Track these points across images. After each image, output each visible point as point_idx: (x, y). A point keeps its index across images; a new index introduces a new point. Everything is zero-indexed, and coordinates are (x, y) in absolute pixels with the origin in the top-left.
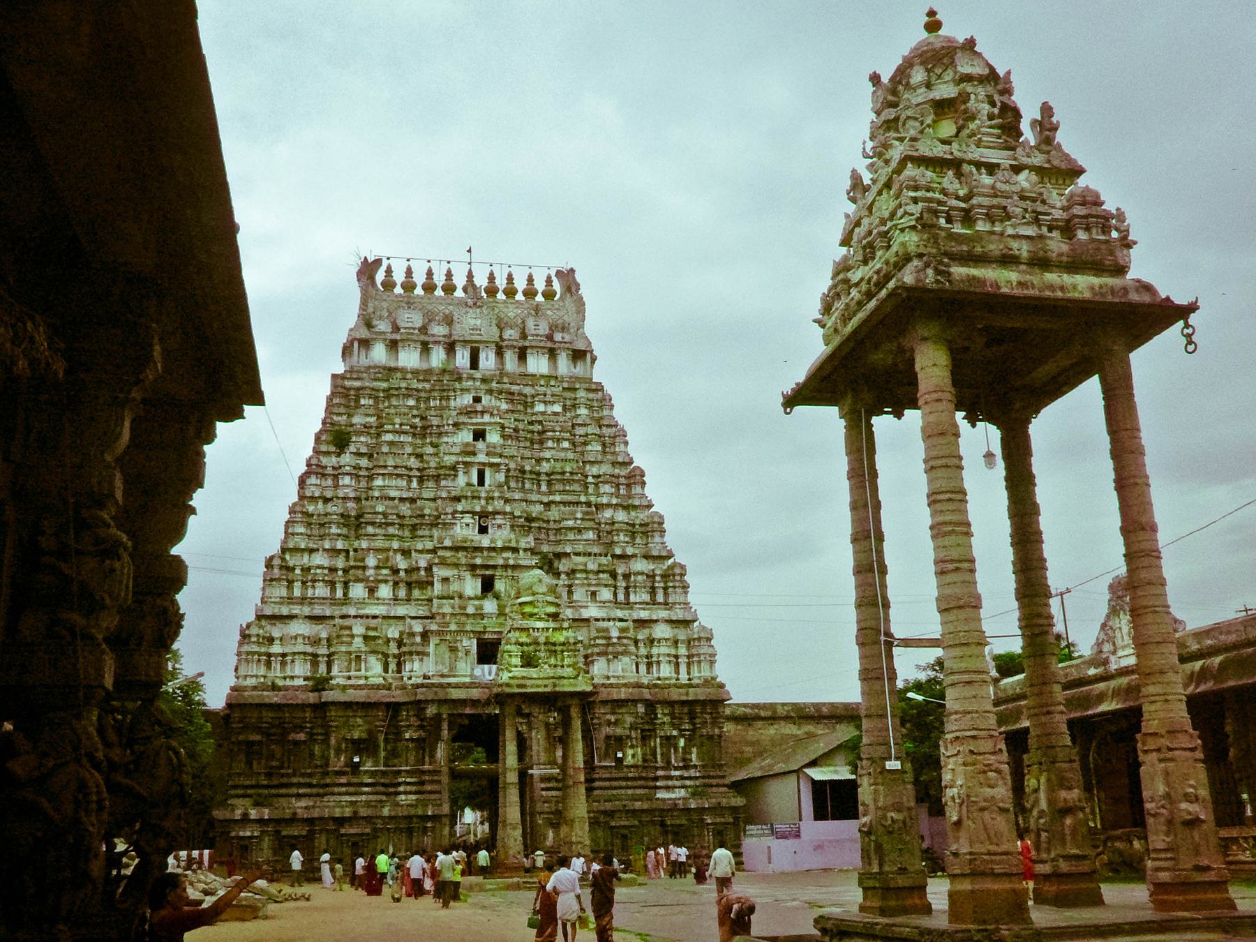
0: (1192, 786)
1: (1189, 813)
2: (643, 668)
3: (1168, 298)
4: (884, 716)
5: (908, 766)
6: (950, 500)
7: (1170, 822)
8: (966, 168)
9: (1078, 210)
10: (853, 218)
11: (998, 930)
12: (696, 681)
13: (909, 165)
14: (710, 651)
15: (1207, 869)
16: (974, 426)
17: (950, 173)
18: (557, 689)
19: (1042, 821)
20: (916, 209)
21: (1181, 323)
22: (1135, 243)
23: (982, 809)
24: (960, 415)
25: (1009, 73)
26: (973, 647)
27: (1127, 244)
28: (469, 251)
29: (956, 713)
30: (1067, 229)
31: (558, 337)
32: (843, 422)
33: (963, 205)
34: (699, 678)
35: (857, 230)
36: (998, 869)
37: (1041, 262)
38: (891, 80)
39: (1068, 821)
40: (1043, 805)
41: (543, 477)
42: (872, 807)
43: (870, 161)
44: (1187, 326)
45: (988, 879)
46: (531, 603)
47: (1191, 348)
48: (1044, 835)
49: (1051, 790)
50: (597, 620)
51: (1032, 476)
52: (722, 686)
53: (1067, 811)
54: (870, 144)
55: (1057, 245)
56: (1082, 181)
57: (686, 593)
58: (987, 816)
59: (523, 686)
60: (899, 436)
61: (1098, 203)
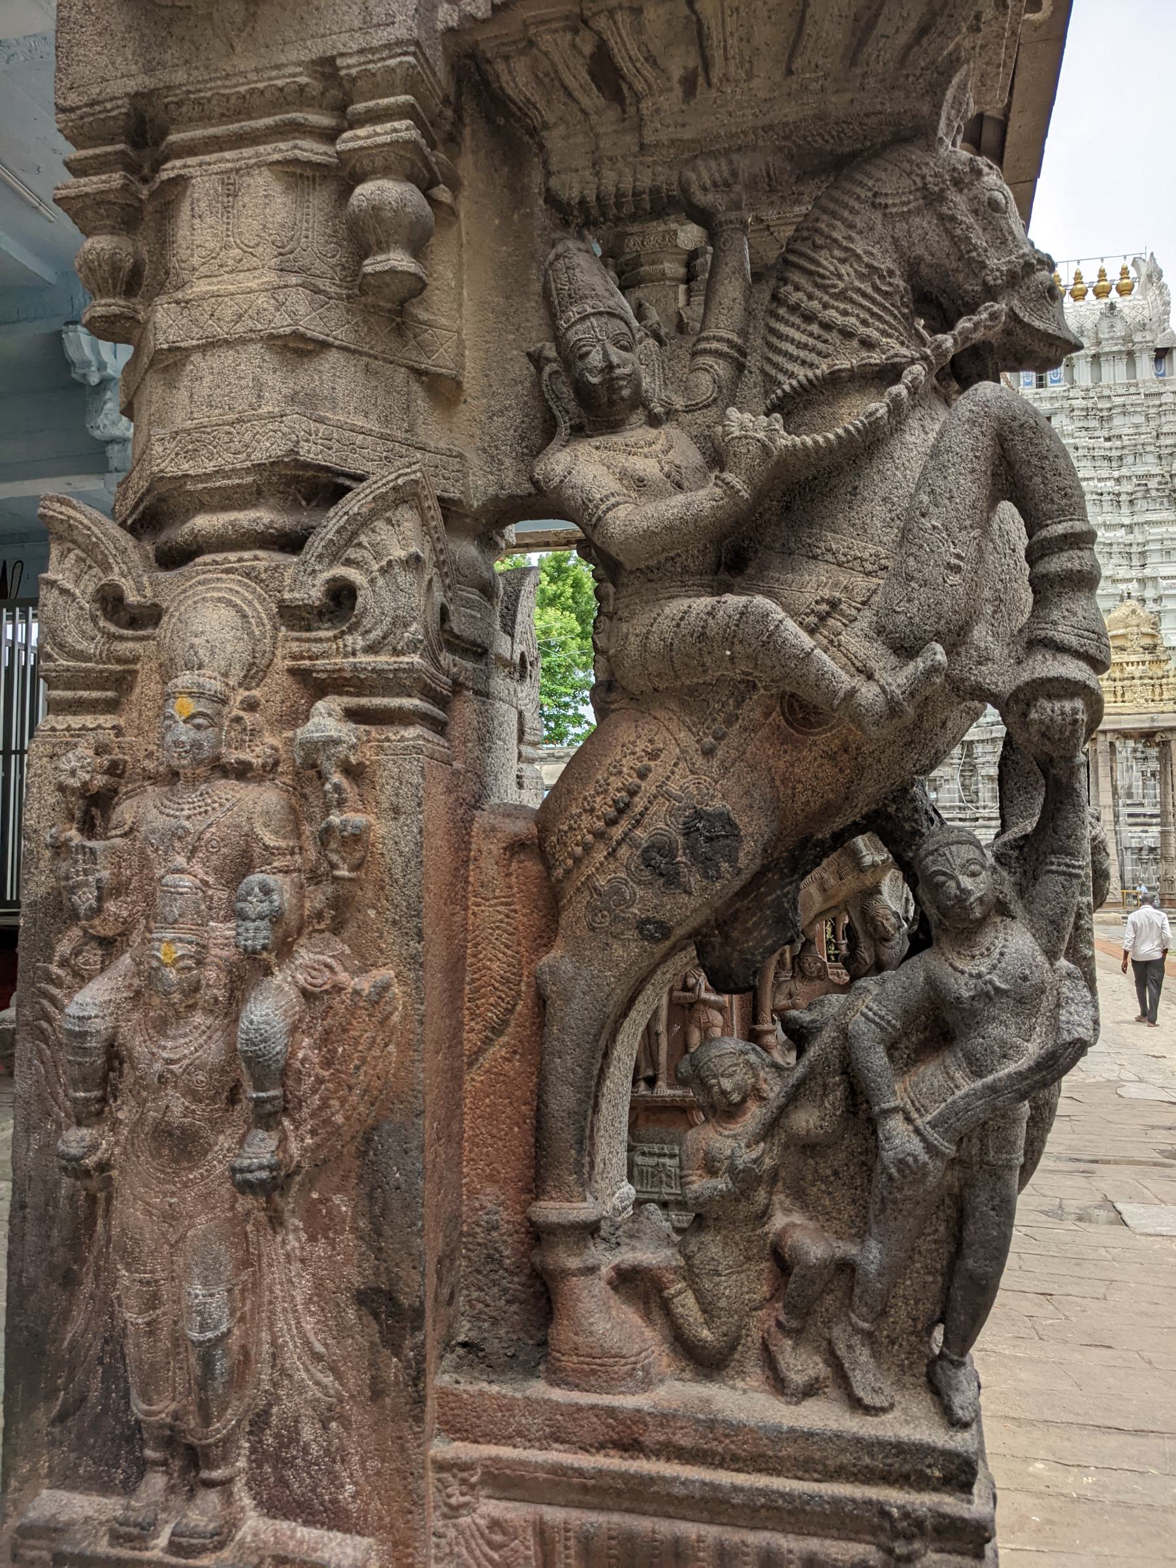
31: (1137, 338)
41: (1123, 497)
46: (1124, 636)
59: (1119, 722)
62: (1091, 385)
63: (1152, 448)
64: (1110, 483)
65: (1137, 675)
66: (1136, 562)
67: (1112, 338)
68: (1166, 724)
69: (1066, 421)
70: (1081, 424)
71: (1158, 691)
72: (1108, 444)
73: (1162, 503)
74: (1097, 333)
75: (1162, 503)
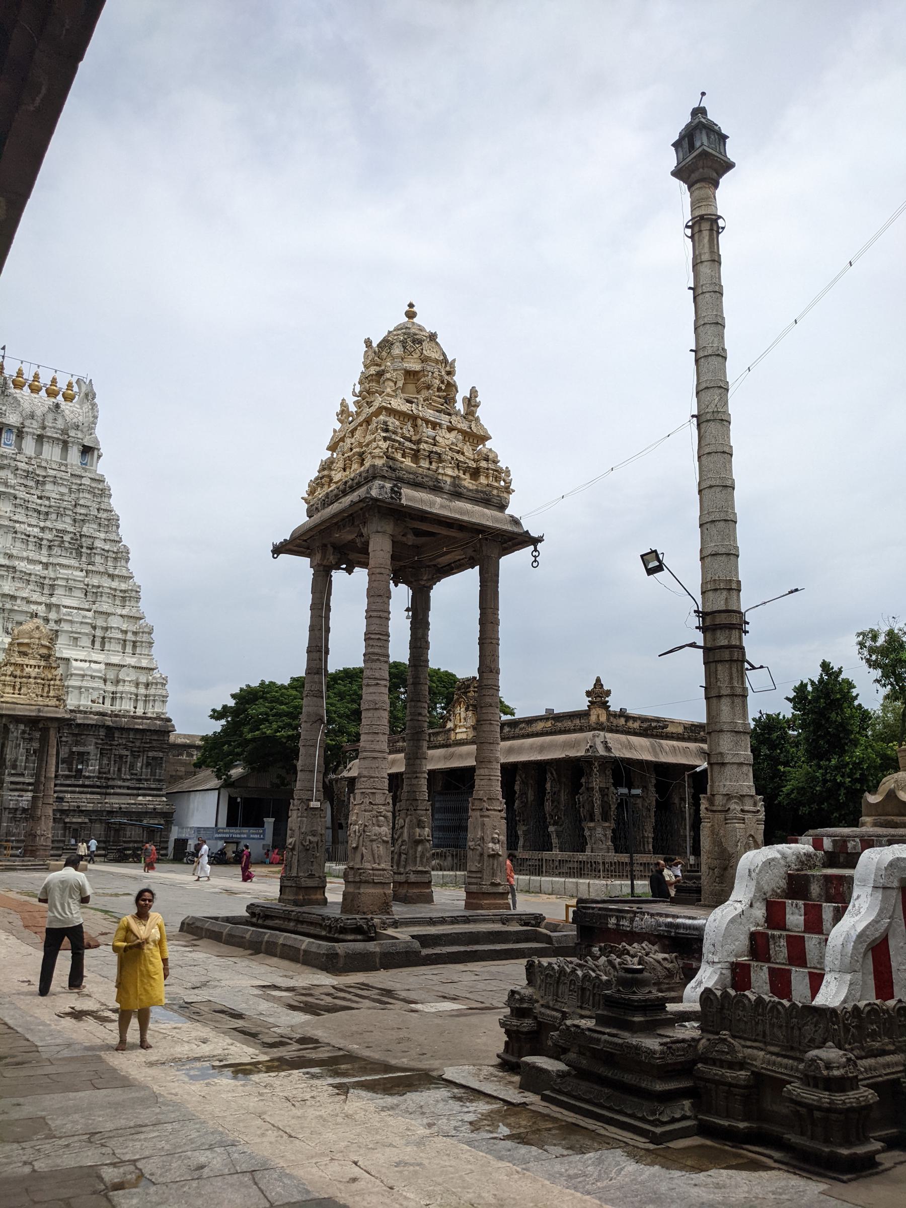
0: (496, 833)
1: (493, 850)
2: (108, 701)
3: (527, 531)
4: (313, 771)
6: (379, 639)
8: (419, 422)
9: (483, 464)
11: (372, 919)
12: (149, 715)
13: (384, 413)
14: (164, 693)
15: (499, 884)
17: (409, 424)
18: (41, 714)
19: (403, 847)
21: (532, 548)
22: (514, 491)
23: (372, 841)
25: (454, 360)
26: (380, 735)
27: (508, 490)
28: (4, 348)
29: (365, 777)
30: (475, 473)
31: (72, 433)
32: (312, 571)
33: (415, 447)
34: (153, 713)
35: (341, 444)
36: (376, 879)
37: (457, 494)
38: (378, 346)
39: (420, 848)
40: (405, 836)
41: (45, 542)
42: (297, 833)
43: (357, 399)
44: (536, 550)
45: (371, 885)
46: (28, 644)
48: (403, 856)
49: (411, 827)
50: (76, 660)
51: (428, 624)
52: (169, 720)
55: (467, 482)
56: (488, 444)
57: (151, 647)
59: (14, 709)
60: (350, 587)
61: (495, 462)
62: (33, 455)
63: (70, 513)
64: (36, 530)
65: (33, 675)
66: (46, 591)
67: (54, 428)
69: (11, 476)
70: (22, 481)
71: (46, 689)
72: (39, 501)
73: (71, 553)
74: (43, 420)
75: (71, 553)
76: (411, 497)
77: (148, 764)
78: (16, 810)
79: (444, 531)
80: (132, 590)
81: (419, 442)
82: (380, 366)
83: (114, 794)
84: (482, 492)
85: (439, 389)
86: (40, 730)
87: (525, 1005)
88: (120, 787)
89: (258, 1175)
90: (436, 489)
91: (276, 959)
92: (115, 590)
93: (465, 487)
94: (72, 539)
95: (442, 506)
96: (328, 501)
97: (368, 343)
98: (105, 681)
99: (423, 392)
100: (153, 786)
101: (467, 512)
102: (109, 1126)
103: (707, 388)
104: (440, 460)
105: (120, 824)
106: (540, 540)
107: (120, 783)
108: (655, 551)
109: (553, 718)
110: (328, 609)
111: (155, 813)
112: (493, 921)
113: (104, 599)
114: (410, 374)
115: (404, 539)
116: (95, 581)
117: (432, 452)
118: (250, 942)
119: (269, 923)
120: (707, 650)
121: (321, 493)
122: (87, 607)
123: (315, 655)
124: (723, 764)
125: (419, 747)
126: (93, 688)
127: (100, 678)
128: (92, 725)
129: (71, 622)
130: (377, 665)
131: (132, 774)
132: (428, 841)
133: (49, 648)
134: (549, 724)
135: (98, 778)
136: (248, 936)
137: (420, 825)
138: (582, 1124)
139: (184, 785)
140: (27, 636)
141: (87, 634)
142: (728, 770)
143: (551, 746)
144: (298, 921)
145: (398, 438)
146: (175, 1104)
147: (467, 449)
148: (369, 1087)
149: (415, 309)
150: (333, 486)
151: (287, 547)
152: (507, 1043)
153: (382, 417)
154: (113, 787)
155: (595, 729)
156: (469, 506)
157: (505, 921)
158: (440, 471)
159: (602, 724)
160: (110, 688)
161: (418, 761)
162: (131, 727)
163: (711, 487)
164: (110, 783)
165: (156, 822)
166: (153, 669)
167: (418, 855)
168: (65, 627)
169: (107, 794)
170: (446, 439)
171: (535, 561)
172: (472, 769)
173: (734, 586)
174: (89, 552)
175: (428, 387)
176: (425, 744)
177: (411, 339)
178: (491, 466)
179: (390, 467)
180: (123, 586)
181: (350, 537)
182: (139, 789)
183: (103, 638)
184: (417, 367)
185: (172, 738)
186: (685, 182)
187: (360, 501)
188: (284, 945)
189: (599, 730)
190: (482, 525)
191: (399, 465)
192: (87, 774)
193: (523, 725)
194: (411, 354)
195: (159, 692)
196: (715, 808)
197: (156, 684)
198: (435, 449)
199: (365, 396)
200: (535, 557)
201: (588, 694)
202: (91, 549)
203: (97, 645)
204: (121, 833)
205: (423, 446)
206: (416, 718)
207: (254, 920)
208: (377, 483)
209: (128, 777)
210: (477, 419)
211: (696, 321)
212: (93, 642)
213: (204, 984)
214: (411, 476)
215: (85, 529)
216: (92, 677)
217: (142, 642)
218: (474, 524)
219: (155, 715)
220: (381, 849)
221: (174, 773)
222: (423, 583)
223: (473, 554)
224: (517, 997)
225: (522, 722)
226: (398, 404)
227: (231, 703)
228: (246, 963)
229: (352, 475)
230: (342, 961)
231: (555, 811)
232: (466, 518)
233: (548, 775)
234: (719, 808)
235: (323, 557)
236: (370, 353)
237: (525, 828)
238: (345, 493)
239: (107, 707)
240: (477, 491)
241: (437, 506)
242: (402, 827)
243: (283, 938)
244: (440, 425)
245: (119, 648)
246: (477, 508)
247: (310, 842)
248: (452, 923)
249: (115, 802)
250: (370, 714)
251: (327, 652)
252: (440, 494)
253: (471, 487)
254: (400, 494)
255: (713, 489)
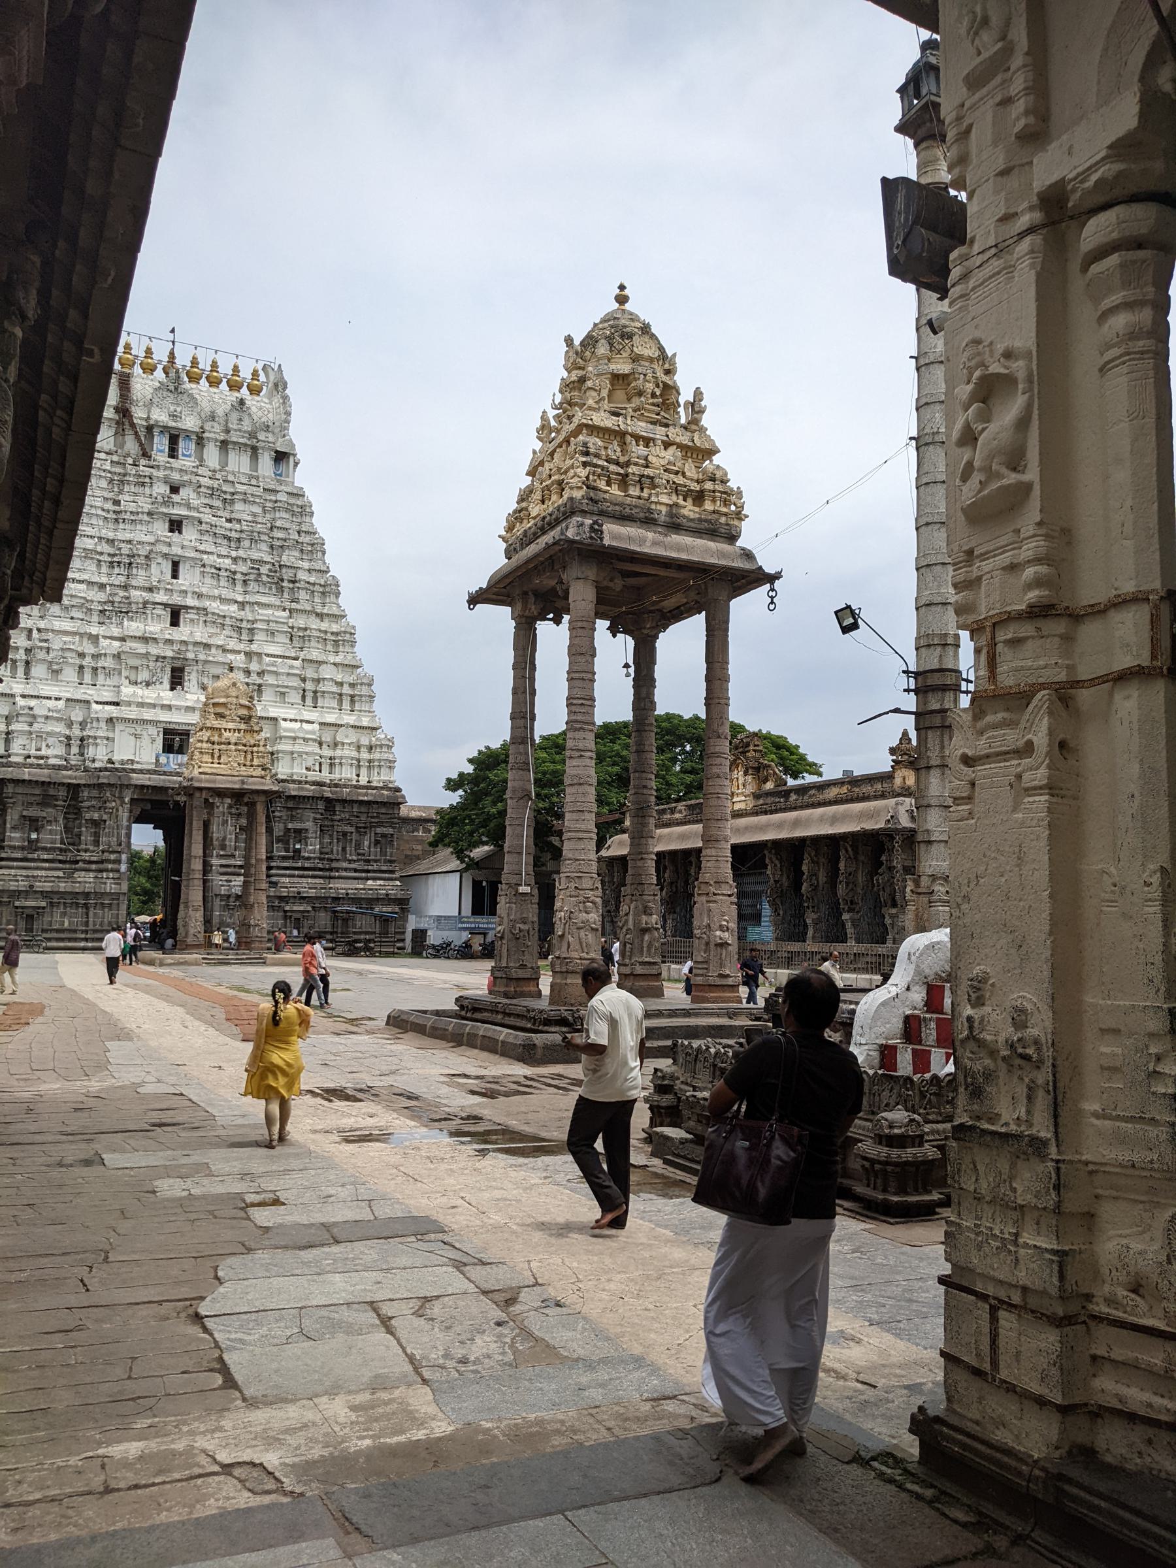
2: (326, 768)
4: (520, 853)
5: (536, 892)
7: (707, 944)
8: (628, 438)
9: (709, 485)
10: (540, 456)
11: (578, 1011)
12: (375, 784)
14: (391, 757)
15: (728, 976)
16: (614, 636)
17: (615, 442)
18: (245, 786)
20: (583, 472)
22: (747, 516)
24: (602, 625)
25: (675, 355)
27: (739, 516)
30: (699, 498)
32: (513, 623)
33: (622, 471)
34: (379, 781)
37: (675, 525)
39: (647, 937)
40: (630, 925)
42: (506, 920)
43: (558, 412)
44: (772, 590)
46: (224, 705)
47: (772, 607)
48: (628, 946)
50: (285, 720)
51: (654, 680)
52: (398, 790)
53: (645, 931)
54: (558, 398)
55: (689, 510)
56: (717, 459)
57: (372, 702)
58: (582, 933)
59: (214, 782)
61: (724, 482)
65: (233, 741)
66: (244, 637)
68: (254, 787)
71: (249, 757)
76: (615, 534)
77: (377, 843)
78: (229, 896)
79: (662, 572)
80: (345, 632)
81: (628, 464)
82: (583, 369)
83: (339, 878)
84: (706, 521)
85: (653, 395)
86: (246, 804)
87: (666, 1082)
88: (346, 870)
89: (373, 1203)
90: (648, 521)
91: (476, 1051)
92: (326, 632)
93: (684, 517)
94: (270, 570)
95: (655, 543)
96: (527, 539)
97: (569, 341)
98: (321, 744)
99: (634, 400)
100: (384, 868)
101: (686, 549)
102: (262, 1169)
103: (927, 404)
104: (654, 486)
105: (348, 912)
106: (777, 576)
107: (345, 865)
108: (849, 607)
109: (849, 783)
110: (533, 668)
111: (388, 900)
112: (718, 1015)
113: (313, 644)
114: (618, 379)
115: (611, 584)
116: (301, 622)
117: (643, 476)
118: (453, 1034)
119: (478, 1015)
120: (918, 715)
121: (519, 529)
122: (293, 655)
123: (521, 722)
124: (930, 842)
125: (644, 825)
126: (307, 753)
127: (315, 740)
128: (309, 797)
129: (276, 673)
130: (580, 734)
131: (359, 854)
132: (657, 929)
133: (249, 708)
134: (844, 790)
135: (320, 859)
136: (450, 1028)
137: (647, 911)
138: (688, 1180)
139: (422, 867)
140: (223, 694)
141: (295, 688)
142: (934, 848)
143: (844, 818)
144: (505, 1014)
145: (600, 462)
146: (323, 1157)
147: (690, 469)
148: (507, 1151)
149: (626, 292)
150: (532, 522)
151: (485, 596)
152: (651, 1119)
153: (581, 438)
154: (337, 870)
155: (899, 795)
156: (688, 540)
157: (732, 1015)
158: (653, 499)
159: (909, 788)
160: (327, 752)
161: (643, 841)
162: (354, 798)
163: (927, 524)
164: (334, 865)
165: (390, 910)
166: (376, 729)
167: (645, 945)
168: (270, 679)
169: (330, 878)
170: (661, 457)
171: (772, 602)
172: (698, 851)
173: (950, 641)
174: (291, 586)
175: (640, 394)
176: (652, 821)
177: (621, 332)
178: (719, 487)
179: (591, 499)
180: (335, 628)
181: (553, 583)
182: (368, 871)
183: (315, 692)
184: (624, 368)
185: (403, 811)
186: (911, 137)
187: (554, 544)
188: (483, 1036)
189: (904, 796)
190: (704, 564)
191: (602, 495)
192: (306, 855)
193: (813, 792)
194: (619, 352)
195: (385, 756)
196: (920, 890)
197: (381, 746)
198: (648, 472)
199: (567, 406)
200: (772, 598)
201: (892, 751)
202: (294, 582)
203: (309, 701)
204: (350, 922)
205: (632, 469)
206: (641, 791)
207: (463, 1013)
208: (577, 519)
209: (355, 858)
210: (702, 430)
211: (918, 320)
212: (304, 697)
213: (393, 1073)
214: (617, 508)
215: (284, 558)
216: (305, 739)
217: (361, 696)
218: (694, 562)
219: (381, 784)
220: (590, 936)
221: (409, 853)
222: (646, 632)
223: (696, 598)
224: (659, 1074)
225: (813, 787)
226: (601, 419)
227: (469, 769)
228: (445, 1053)
229: (551, 509)
230: (540, 1052)
231: (851, 895)
232: (683, 556)
233: (842, 853)
234: (924, 890)
235: (525, 608)
236: (571, 354)
237: (815, 916)
238: (544, 531)
239: (325, 776)
240: (700, 520)
241: (648, 544)
242: (627, 914)
243: (483, 1029)
244: (654, 440)
245: (335, 704)
246: (699, 541)
247: (520, 930)
248: (670, 1016)
249: (341, 887)
250: (573, 790)
251: (533, 719)
252: (654, 528)
253: (692, 515)
254: (602, 532)
255: (930, 527)
